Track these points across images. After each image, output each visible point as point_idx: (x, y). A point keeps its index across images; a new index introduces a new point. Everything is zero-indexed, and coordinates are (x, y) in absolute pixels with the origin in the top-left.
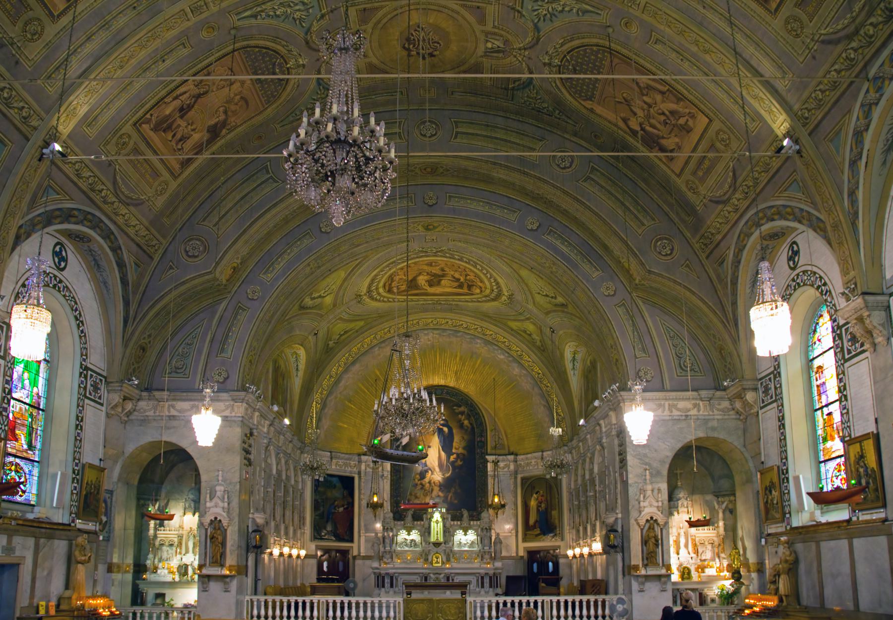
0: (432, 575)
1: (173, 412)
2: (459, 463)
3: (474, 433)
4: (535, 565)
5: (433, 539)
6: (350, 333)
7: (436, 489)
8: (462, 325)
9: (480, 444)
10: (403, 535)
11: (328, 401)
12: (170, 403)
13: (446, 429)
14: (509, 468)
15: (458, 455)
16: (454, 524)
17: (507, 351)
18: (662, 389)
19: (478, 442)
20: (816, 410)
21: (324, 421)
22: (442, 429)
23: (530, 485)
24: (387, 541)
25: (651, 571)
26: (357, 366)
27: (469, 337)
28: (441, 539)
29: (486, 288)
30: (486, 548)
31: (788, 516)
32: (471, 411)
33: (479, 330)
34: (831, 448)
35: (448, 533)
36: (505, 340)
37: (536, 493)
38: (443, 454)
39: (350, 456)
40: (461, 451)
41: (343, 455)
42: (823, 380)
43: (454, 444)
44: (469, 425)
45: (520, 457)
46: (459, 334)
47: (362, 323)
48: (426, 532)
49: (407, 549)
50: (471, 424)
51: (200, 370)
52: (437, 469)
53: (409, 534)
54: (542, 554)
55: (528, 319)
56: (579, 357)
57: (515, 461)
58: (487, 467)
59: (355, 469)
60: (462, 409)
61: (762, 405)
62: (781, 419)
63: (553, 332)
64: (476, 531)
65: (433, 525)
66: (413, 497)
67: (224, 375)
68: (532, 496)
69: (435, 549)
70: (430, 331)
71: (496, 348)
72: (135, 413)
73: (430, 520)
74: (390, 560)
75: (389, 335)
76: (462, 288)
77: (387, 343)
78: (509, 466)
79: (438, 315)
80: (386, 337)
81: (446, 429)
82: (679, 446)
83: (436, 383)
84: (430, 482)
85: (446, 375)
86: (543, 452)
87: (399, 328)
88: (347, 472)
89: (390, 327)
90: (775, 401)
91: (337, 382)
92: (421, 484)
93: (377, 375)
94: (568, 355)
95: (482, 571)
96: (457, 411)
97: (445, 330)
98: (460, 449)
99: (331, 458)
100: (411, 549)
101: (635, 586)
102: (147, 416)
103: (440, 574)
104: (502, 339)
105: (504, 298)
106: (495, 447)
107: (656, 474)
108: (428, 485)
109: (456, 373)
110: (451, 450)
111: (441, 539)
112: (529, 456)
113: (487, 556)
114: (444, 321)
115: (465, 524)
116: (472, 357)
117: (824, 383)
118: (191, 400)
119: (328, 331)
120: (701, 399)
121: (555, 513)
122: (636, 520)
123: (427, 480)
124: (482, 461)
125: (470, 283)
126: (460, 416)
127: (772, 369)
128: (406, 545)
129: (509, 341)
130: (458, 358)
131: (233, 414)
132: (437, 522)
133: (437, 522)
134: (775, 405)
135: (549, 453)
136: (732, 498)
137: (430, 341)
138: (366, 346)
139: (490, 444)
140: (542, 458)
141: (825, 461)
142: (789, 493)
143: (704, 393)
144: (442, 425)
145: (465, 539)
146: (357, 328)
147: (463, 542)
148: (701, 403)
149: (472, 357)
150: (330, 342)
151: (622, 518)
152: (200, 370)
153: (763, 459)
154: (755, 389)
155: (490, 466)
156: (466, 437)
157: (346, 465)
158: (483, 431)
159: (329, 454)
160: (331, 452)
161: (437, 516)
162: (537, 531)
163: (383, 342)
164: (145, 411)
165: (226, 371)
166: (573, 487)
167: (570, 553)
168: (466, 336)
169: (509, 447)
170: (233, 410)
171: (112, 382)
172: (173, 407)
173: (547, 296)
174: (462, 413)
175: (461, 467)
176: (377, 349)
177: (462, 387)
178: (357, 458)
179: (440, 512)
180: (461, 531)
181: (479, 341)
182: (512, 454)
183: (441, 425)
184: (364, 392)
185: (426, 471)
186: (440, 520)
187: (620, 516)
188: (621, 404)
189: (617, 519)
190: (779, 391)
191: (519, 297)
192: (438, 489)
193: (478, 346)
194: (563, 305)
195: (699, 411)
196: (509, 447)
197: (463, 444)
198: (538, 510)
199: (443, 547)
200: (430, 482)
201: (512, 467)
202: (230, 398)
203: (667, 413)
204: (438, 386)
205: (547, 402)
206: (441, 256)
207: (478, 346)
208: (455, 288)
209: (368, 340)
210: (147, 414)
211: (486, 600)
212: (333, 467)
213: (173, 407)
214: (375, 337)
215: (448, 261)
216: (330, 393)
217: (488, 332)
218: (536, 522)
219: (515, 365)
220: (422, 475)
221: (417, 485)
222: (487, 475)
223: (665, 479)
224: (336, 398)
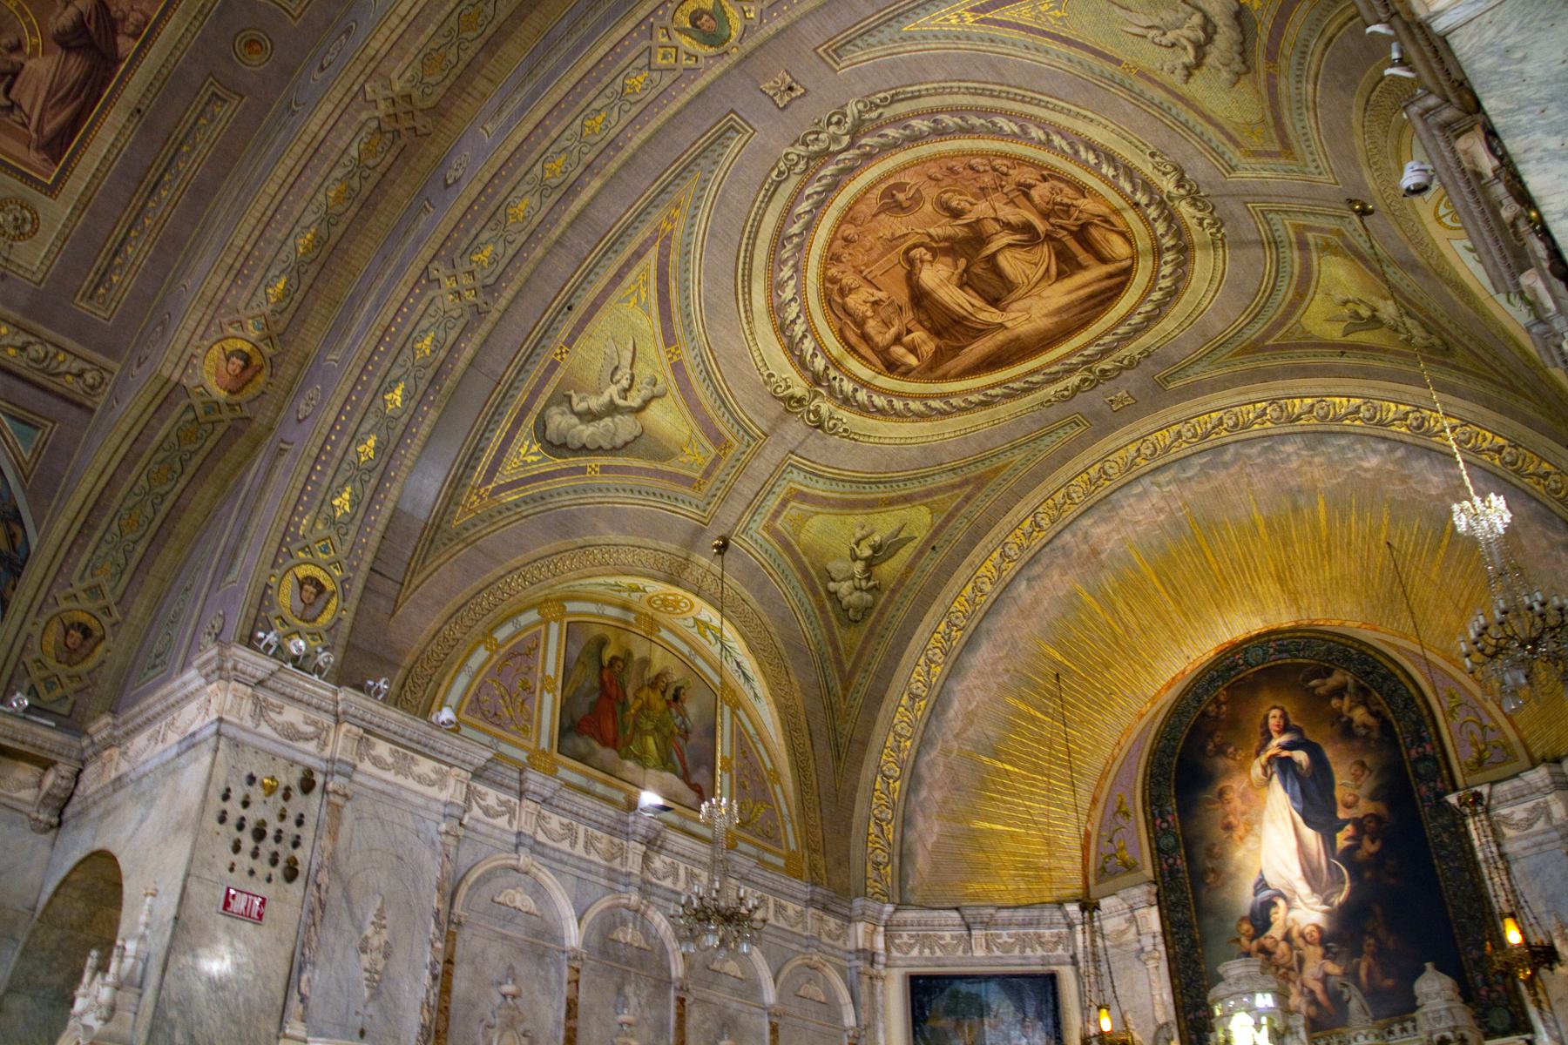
2: (1369, 847)
3: (1394, 737)
6: (905, 553)
7: (1313, 953)
9: (1421, 768)
11: (924, 770)
13: (1300, 756)
14: (1549, 817)
15: (1358, 823)
17: (1377, 433)
19: (1417, 761)
21: (920, 822)
22: (1289, 759)
26: (984, 654)
27: (1254, 451)
29: (1117, 212)
32: (1367, 674)
36: (1355, 402)
38: (1311, 836)
39: (1035, 913)
40: (1365, 808)
41: (1005, 914)
43: (1339, 793)
44: (1371, 721)
46: (1228, 456)
47: (919, 519)
52: (1303, 888)
58: (1467, 834)
59: (1060, 951)
60: (1336, 679)
71: (1343, 442)
75: (1040, 538)
76: (1080, 267)
77: (1045, 561)
79: (1146, 424)
80: (1036, 544)
81: (1300, 756)
84: (1287, 937)
85: (1255, 598)
87: (1059, 508)
88: (1032, 959)
89: (1034, 512)
91: (939, 706)
92: (1263, 950)
93: (1054, 662)
96: (1321, 691)
98: (1362, 802)
99: (969, 929)
104: (1342, 405)
105: (1185, 209)
106: (1480, 762)
108: (1283, 946)
109: (1281, 580)
110: (1334, 813)
114: (1166, 437)
116: (1296, 509)
119: (787, 546)
123: (1276, 932)
124: (1445, 820)
126: (1335, 702)
129: (1367, 399)
130: (1262, 529)
131: (207, 720)
137: (1161, 510)
138: (987, 588)
144: (1290, 746)
146: (922, 535)
149: (1296, 509)
150: (832, 586)
156: (1368, 760)
157: (1023, 942)
158: (1419, 722)
159: (955, 914)
160: (957, 909)
163: (1034, 560)
165: (223, 617)
168: (1248, 451)
174: (1340, 692)
175: (1377, 860)
178: (1057, 915)
181: (1289, 448)
183: (1284, 748)
184: (1033, 719)
185: (1269, 905)
191: (1199, 169)
192: (1319, 951)
193: (1294, 465)
196: (1526, 748)
197: (1368, 784)
200: (1287, 937)
202: (203, 681)
204: (1251, 639)
207: (1294, 465)
212: (979, 953)
214: (1004, 555)
215: (920, 162)
216: (924, 743)
217: (1298, 406)
219: (1420, 465)
220: (1261, 919)
224: (946, 753)
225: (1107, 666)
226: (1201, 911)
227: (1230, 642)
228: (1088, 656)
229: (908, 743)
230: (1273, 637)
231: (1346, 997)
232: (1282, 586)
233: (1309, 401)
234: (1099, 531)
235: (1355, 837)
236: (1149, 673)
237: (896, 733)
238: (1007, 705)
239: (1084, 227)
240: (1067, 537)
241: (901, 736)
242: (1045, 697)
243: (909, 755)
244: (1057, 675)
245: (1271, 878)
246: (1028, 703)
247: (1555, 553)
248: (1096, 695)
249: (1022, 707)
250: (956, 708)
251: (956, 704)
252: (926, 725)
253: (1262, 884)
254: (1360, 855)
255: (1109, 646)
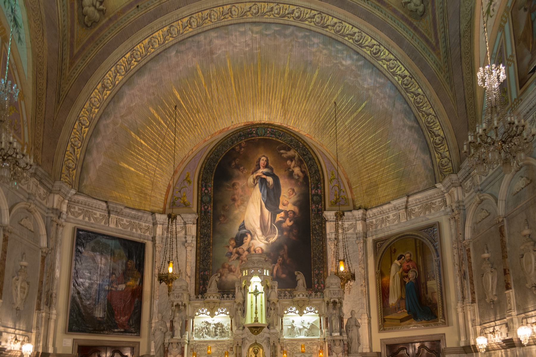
8: (292, 12)
66: (226, 270)
70: (248, 27)
83: (257, 120)
91: (116, 97)
132: (256, 293)
133: (256, 293)
161: (256, 283)
169: (353, 201)
176: (174, 53)
179: (261, 275)
186: (261, 288)
204: (260, 124)
205: (416, 121)
221: (231, 253)
222: (326, 238)
225: (198, 112)
227: (251, 122)
228: (192, 103)
229: (97, 110)
230: (270, 127)
231: (297, 278)
232: (282, 106)
236: (215, 123)
237: (91, 102)
238: (150, 111)
241: (93, 105)
242: (168, 115)
243: (95, 117)
244: (176, 106)
246: (159, 115)
247: (404, 129)
248: (189, 123)
249: (156, 115)
250: (124, 102)
251: (125, 100)
252: (108, 105)
255: (202, 102)
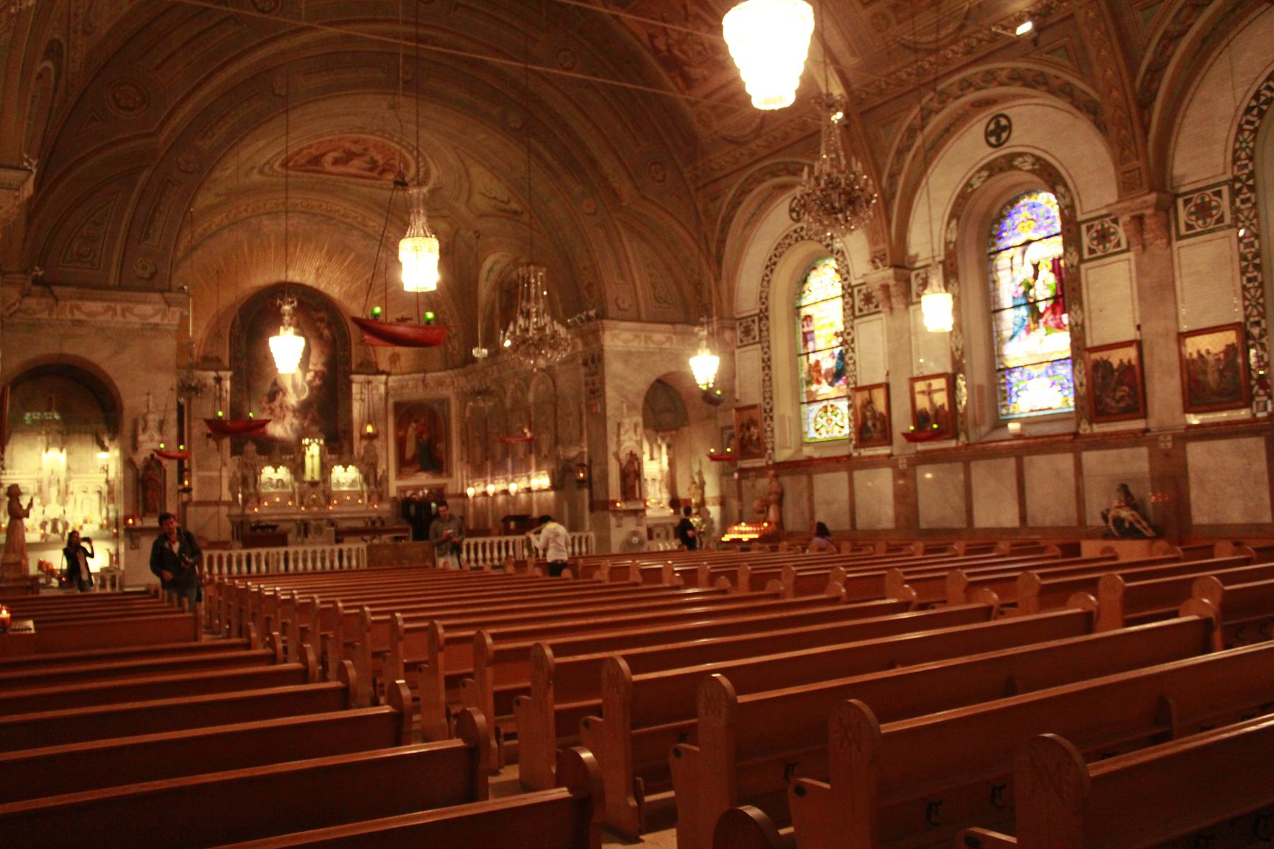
0: (313, 523)
1: (78, 316)
2: (318, 382)
4: (413, 509)
5: (308, 477)
10: (268, 473)
12: (74, 302)
16: (331, 459)
18: (638, 320)
20: (800, 355)
23: (405, 412)
24: (251, 481)
25: (631, 506)
26: (199, 252)
28: (317, 478)
30: (373, 487)
31: (770, 451)
33: (360, 219)
34: (817, 391)
35: (325, 468)
37: (416, 421)
42: (811, 328)
45: (391, 379)
46: (333, 222)
48: (298, 468)
49: (272, 490)
50: (332, 334)
51: (115, 259)
53: (276, 472)
54: (421, 493)
55: (444, 217)
56: (497, 268)
57: (386, 383)
61: (739, 344)
62: (767, 364)
63: (478, 237)
64: (358, 466)
65: (308, 460)
67: (150, 269)
68: (409, 424)
69: (312, 490)
72: (20, 315)
73: (304, 454)
74: (255, 504)
75: (244, 215)
78: (377, 388)
82: (653, 379)
84: (281, 406)
86: (425, 372)
90: (760, 342)
94: (488, 264)
95: (375, 515)
97: (315, 215)
100: (278, 490)
101: (613, 521)
102: (39, 319)
103: (322, 519)
107: (632, 407)
109: (318, 270)
111: (317, 478)
112: (406, 377)
113: (375, 497)
114: (316, 204)
115: (346, 459)
117: (812, 332)
118: (106, 300)
120: (675, 333)
121: (441, 446)
122: (617, 455)
123: (277, 403)
125: (387, 167)
126: (318, 324)
127: (757, 311)
128: (272, 485)
131: (166, 321)
133: (312, 456)
134: (759, 346)
135: (434, 374)
136: (674, 433)
138: (213, 227)
139: (355, 361)
140: (423, 381)
141: (809, 403)
142: (772, 430)
143: (679, 327)
145: (345, 476)
147: (342, 481)
148: (674, 337)
149: (342, 252)
151: (589, 453)
152: (115, 259)
153: (737, 396)
154: (733, 329)
155: (355, 388)
162: (418, 466)
164: (35, 312)
166: (467, 415)
167: (470, 492)
170: (164, 315)
171: (10, 272)
172: (79, 309)
173: (495, 198)
174: (321, 320)
175: (319, 388)
176: (226, 231)
177: (322, 286)
179: (318, 444)
180: (340, 467)
181: (356, 233)
182: (382, 373)
187: (586, 449)
188: (601, 333)
189: (581, 454)
190: (764, 334)
194: (515, 212)
195: (672, 344)
197: (323, 359)
198: (418, 443)
199: (321, 486)
200: (281, 406)
201: (382, 388)
203: (643, 344)
206: (378, 136)
208: (364, 170)
209: (217, 219)
210: (38, 316)
211: (310, 549)
213: (79, 309)
214: (227, 216)
218: (414, 456)
223: (641, 412)
226: (249, 389)
233: (374, 224)
234: (266, 222)
235: (314, 378)
239: (389, 170)
240: (253, 220)
245: (279, 382)
253: (275, 384)
254: (314, 384)
